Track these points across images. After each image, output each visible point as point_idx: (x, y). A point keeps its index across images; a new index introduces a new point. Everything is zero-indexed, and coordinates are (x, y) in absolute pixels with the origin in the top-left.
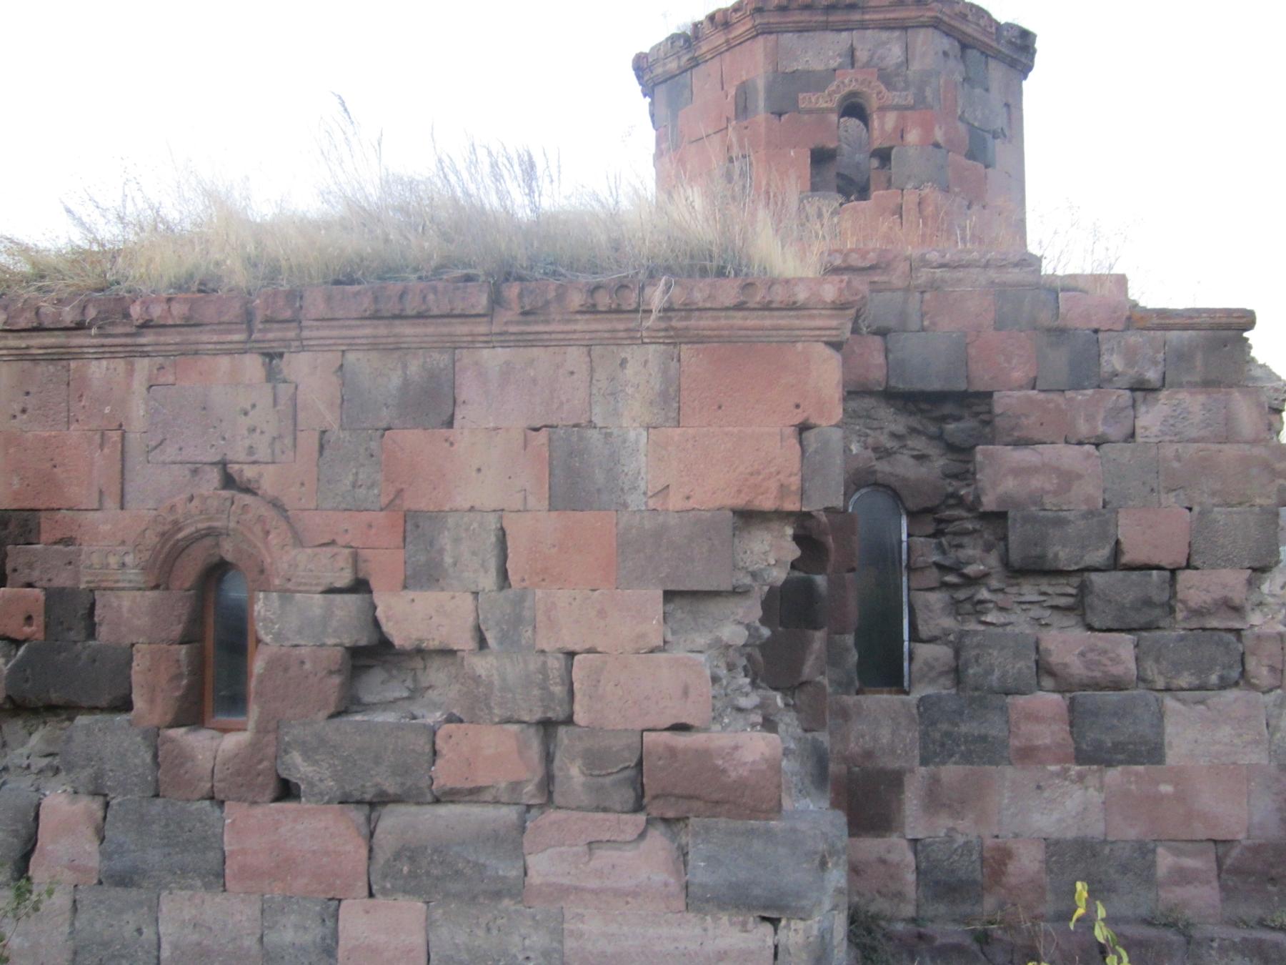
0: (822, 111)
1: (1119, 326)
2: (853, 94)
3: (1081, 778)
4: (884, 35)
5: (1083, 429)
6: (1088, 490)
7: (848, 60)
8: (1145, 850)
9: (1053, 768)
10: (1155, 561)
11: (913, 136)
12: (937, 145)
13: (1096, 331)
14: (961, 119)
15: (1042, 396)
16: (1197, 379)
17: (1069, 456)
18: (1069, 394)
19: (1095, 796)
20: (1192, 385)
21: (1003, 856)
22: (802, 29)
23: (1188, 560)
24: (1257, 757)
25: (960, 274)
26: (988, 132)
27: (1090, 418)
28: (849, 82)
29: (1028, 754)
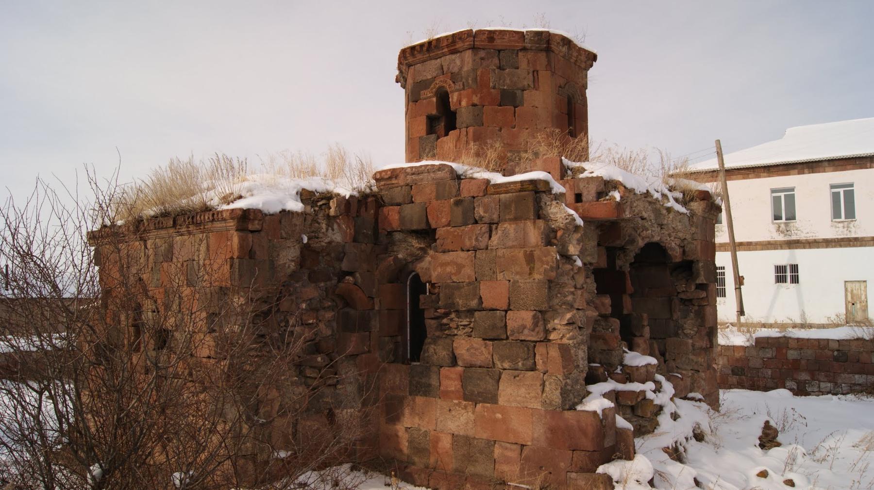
0: (430, 97)
1: (481, 194)
2: (441, 87)
3: (465, 407)
4: (453, 56)
5: (468, 243)
6: (468, 272)
7: (440, 72)
8: (491, 444)
9: (456, 401)
10: (494, 307)
11: (464, 103)
12: (474, 105)
13: (474, 197)
14: (494, 88)
15: (452, 229)
16: (512, 217)
17: (461, 257)
18: (463, 228)
19: (472, 417)
20: (510, 220)
21: (437, 441)
22: (423, 62)
23: (509, 305)
24: (537, 406)
25: (421, 177)
26: (518, 89)
27: (470, 239)
28: (438, 82)
29: (446, 395)
